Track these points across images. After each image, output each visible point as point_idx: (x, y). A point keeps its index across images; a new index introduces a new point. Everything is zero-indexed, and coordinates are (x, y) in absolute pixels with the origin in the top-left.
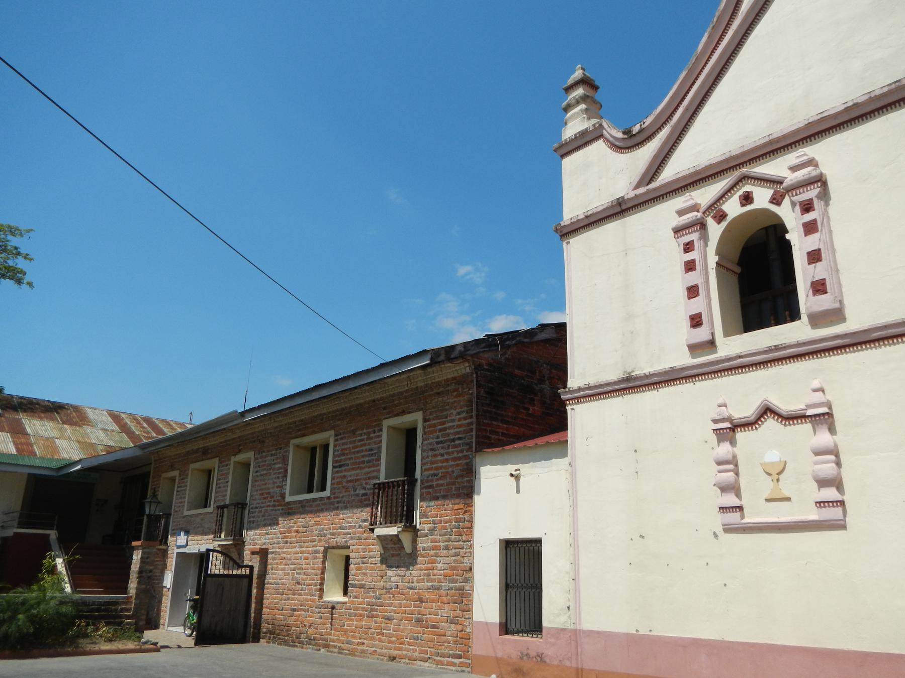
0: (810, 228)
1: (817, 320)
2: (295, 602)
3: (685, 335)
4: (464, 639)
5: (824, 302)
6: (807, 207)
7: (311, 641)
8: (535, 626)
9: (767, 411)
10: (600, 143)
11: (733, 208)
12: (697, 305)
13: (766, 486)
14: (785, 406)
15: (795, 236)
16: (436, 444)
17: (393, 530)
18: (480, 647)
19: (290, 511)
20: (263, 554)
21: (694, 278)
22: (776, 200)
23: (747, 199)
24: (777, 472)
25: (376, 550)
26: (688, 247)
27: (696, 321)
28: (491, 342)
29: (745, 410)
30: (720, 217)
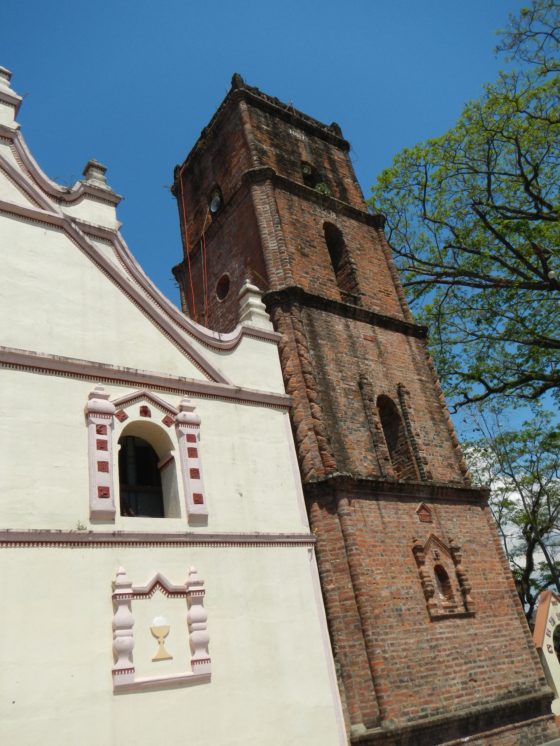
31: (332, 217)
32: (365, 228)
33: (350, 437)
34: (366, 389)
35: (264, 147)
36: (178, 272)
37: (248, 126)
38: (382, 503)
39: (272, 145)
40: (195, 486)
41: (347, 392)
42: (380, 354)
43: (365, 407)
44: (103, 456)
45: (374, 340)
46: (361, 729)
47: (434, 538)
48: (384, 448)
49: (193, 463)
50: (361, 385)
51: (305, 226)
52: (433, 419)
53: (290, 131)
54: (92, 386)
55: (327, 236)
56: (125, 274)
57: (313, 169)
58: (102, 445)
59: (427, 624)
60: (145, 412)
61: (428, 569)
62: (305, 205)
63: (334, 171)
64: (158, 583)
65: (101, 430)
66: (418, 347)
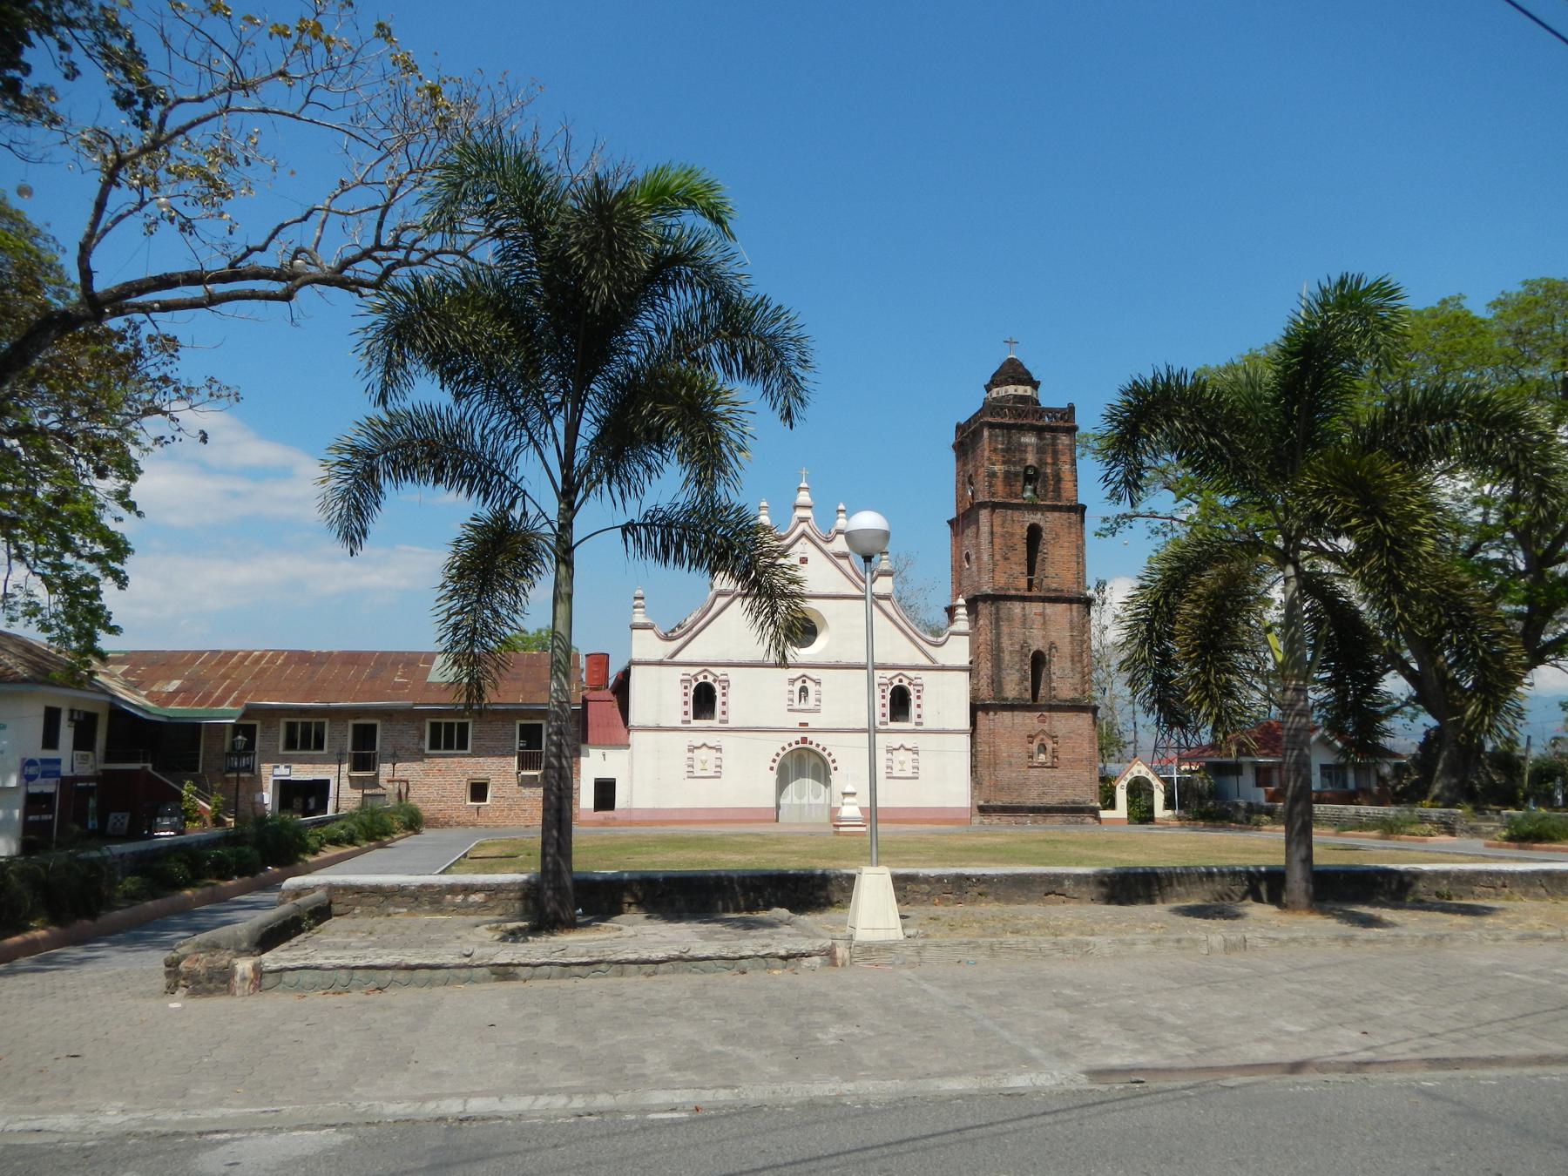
0: (724, 695)
1: (721, 722)
2: (442, 805)
3: (681, 717)
5: (724, 717)
6: (724, 688)
7: (458, 824)
9: (704, 745)
10: (651, 632)
11: (701, 679)
13: (701, 766)
15: (718, 694)
17: (536, 773)
19: (429, 756)
20: (407, 782)
22: (715, 681)
23: (705, 677)
24: (704, 762)
26: (686, 688)
27: (686, 713)
30: (696, 680)
31: (1037, 518)
32: (1065, 515)
33: (1008, 678)
34: (1026, 650)
35: (996, 468)
36: (951, 523)
37: (986, 453)
39: (1004, 463)
40: (919, 711)
41: (1011, 652)
42: (1044, 623)
45: (1043, 615)
46: (981, 803)
47: (1043, 731)
48: (1028, 684)
49: (919, 702)
50: (1022, 647)
51: (1012, 535)
52: (1072, 661)
53: (1023, 439)
55: (1028, 538)
56: (895, 616)
57: (1036, 470)
60: (901, 681)
61: (1035, 747)
62: (1017, 515)
63: (1054, 463)
64: (902, 746)
66: (1078, 612)
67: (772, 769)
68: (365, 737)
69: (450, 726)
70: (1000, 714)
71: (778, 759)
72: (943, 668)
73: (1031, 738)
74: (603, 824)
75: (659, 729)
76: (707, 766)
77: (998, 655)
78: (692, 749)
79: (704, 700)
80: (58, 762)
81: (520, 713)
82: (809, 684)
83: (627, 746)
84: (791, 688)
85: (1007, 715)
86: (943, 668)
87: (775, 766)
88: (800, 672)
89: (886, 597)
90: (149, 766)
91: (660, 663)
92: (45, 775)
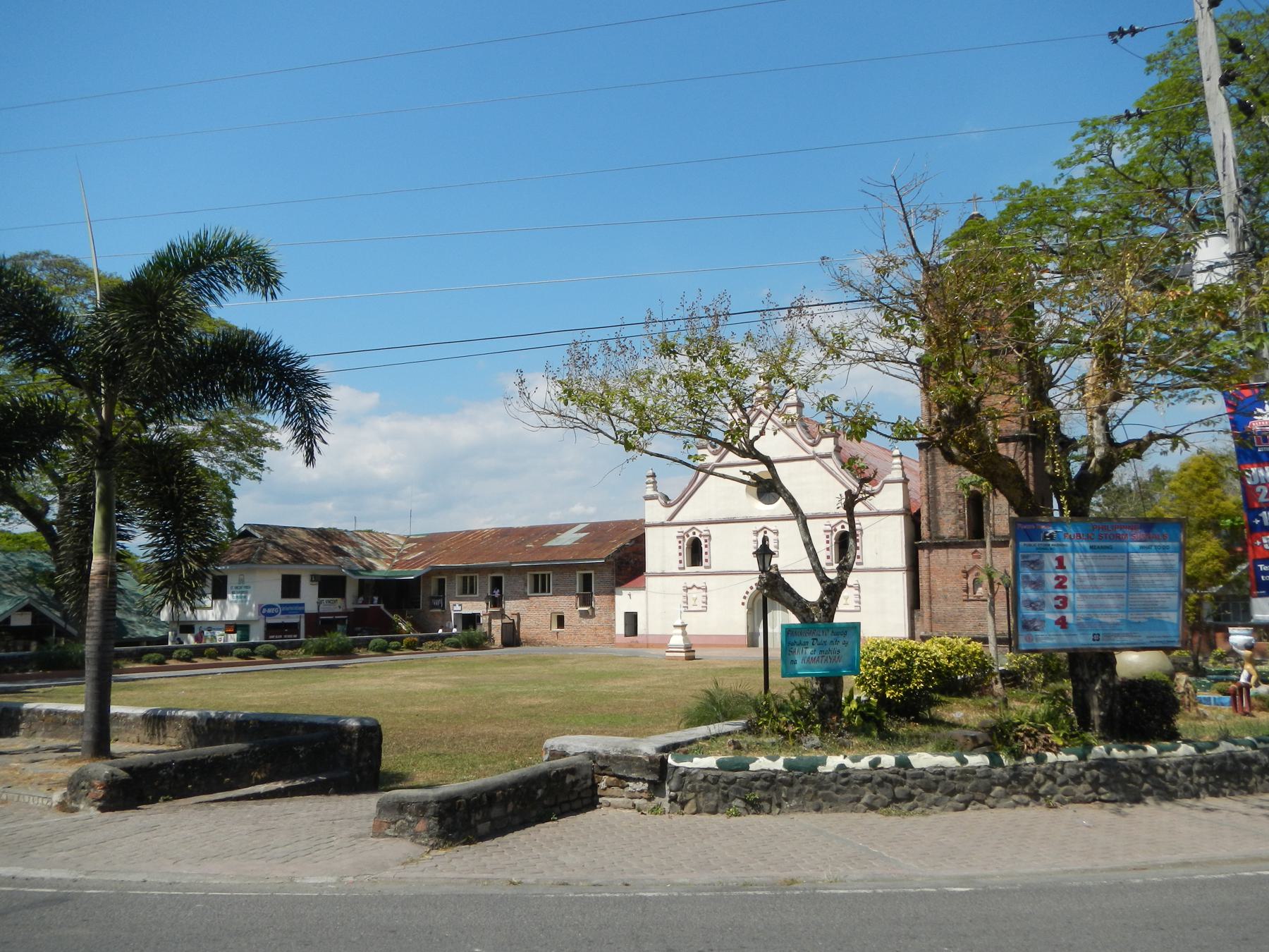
0: (706, 546)
2: (538, 631)
3: (677, 565)
4: (612, 641)
5: (707, 564)
7: (547, 644)
8: (635, 633)
9: (694, 586)
11: (691, 534)
12: (681, 558)
14: (698, 585)
15: (703, 546)
16: (585, 575)
18: (617, 641)
21: (681, 551)
23: (694, 533)
25: (578, 615)
27: (680, 562)
28: (618, 550)
29: (690, 586)
38: (950, 550)
43: (957, 501)
44: (829, 545)
54: (825, 521)
58: (828, 542)
59: (961, 602)
65: (827, 537)
67: (743, 604)
68: (497, 583)
69: (543, 576)
70: (934, 552)
71: (748, 596)
72: (879, 514)
73: (966, 574)
74: (630, 646)
75: (663, 574)
76: (697, 603)
77: (934, 498)
78: (687, 589)
79: (695, 552)
80: (303, 605)
81: (579, 567)
82: (769, 534)
83: (644, 588)
84: (755, 538)
85: (942, 552)
86: (879, 514)
87: (746, 601)
88: (759, 525)
89: (828, 456)
90: (382, 606)
91: (662, 525)
92: (283, 613)
